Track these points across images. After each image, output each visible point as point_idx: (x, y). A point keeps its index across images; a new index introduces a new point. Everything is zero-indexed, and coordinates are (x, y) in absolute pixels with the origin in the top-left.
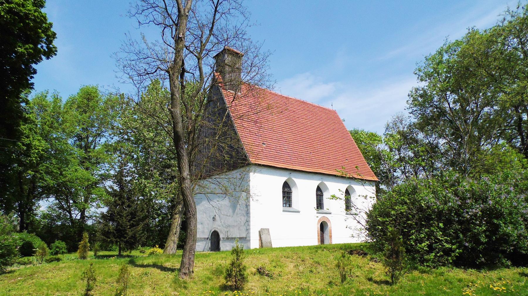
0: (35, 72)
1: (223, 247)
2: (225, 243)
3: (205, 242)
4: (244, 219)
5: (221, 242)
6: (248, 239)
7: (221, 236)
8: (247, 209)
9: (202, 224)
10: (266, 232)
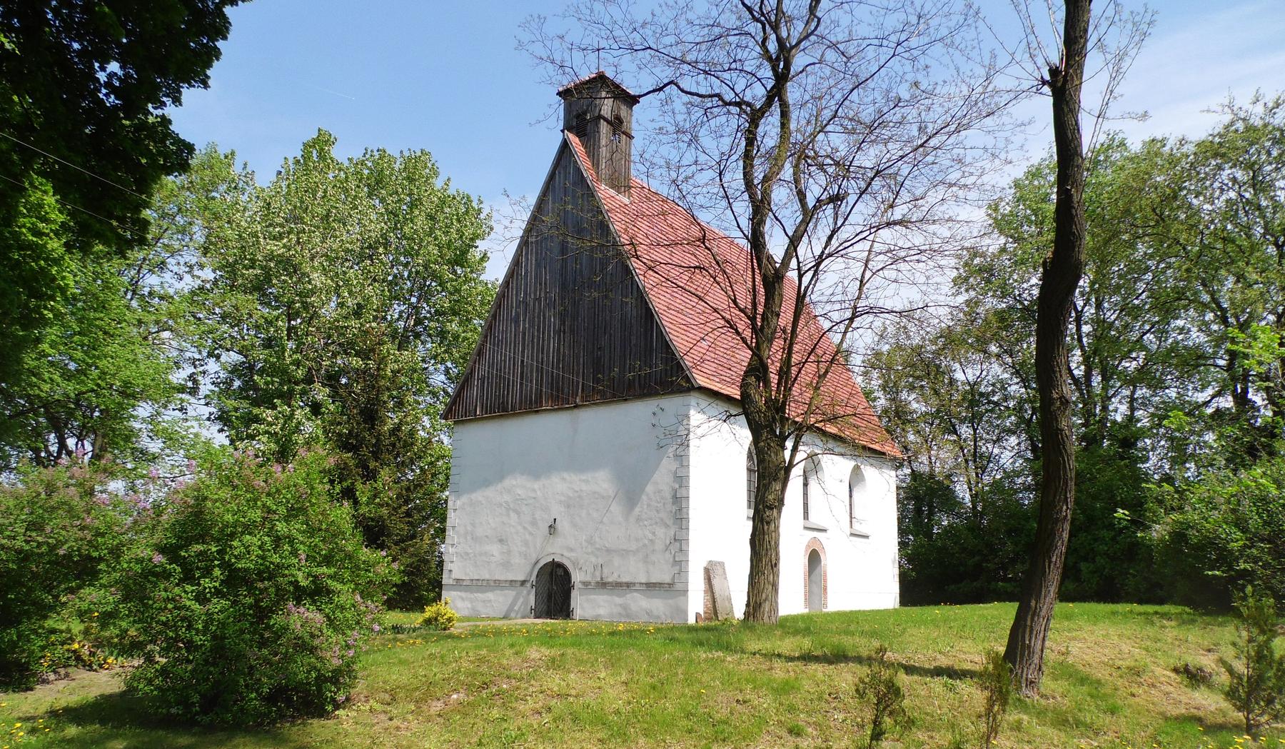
0: (237, 5)
1: (582, 608)
2: (592, 597)
3: (511, 594)
4: (663, 535)
5: (574, 594)
6: (678, 586)
7: (577, 577)
8: (674, 508)
9: (501, 541)
10: (720, 571)
